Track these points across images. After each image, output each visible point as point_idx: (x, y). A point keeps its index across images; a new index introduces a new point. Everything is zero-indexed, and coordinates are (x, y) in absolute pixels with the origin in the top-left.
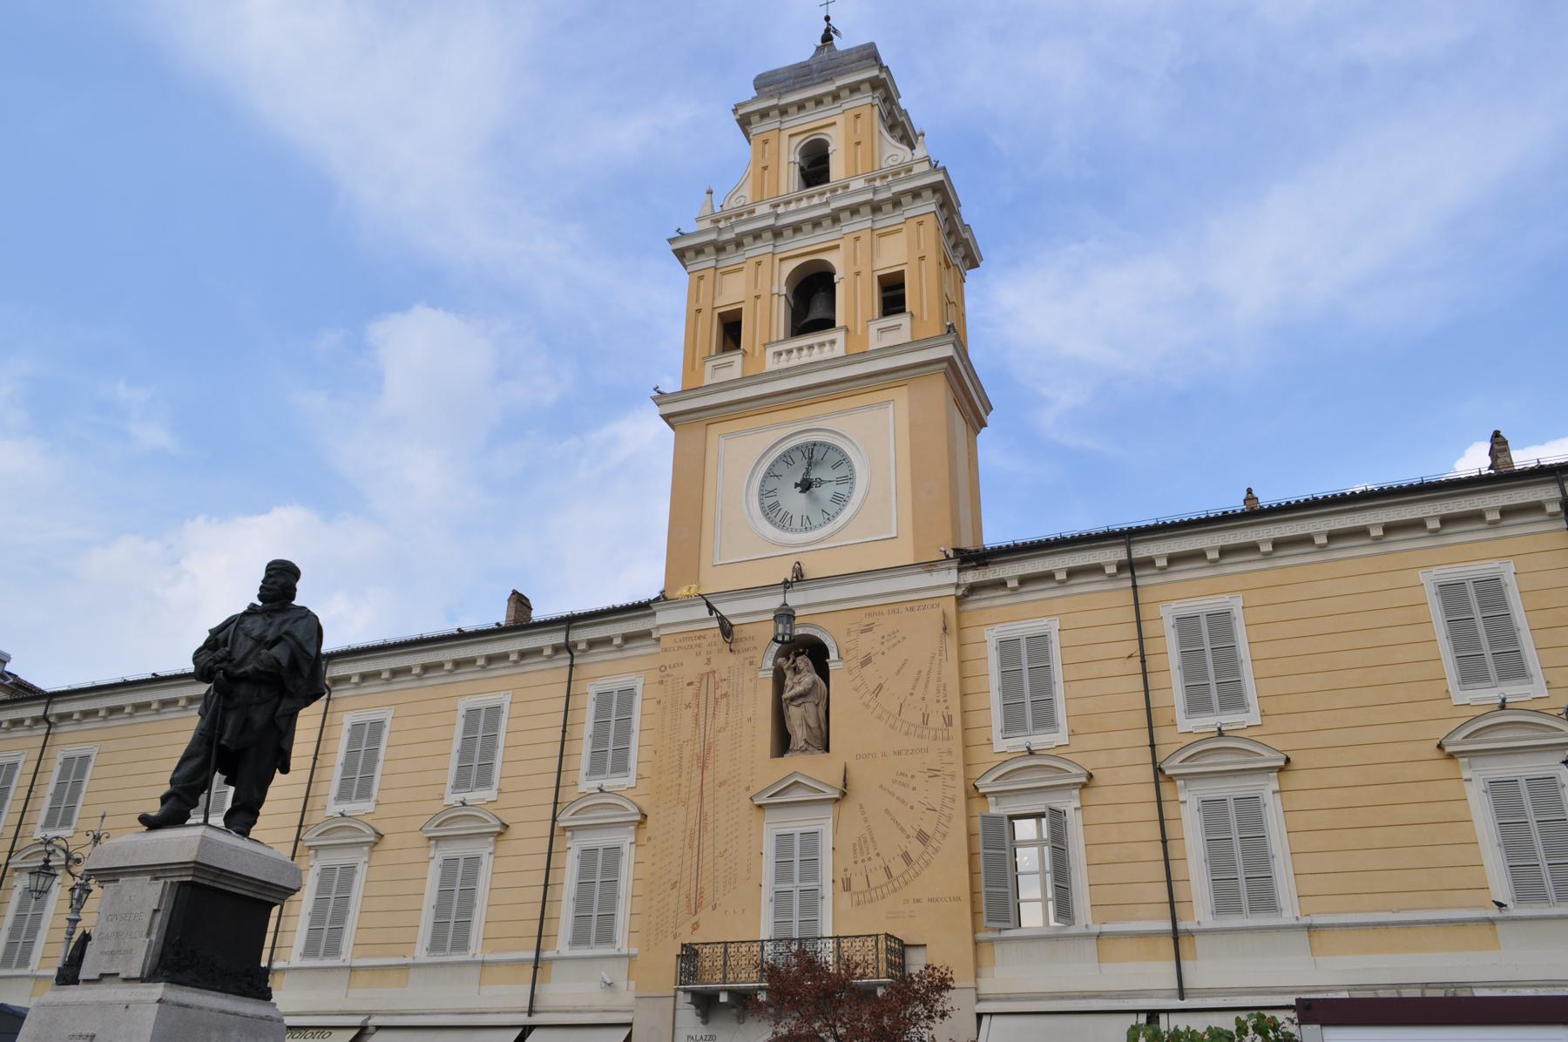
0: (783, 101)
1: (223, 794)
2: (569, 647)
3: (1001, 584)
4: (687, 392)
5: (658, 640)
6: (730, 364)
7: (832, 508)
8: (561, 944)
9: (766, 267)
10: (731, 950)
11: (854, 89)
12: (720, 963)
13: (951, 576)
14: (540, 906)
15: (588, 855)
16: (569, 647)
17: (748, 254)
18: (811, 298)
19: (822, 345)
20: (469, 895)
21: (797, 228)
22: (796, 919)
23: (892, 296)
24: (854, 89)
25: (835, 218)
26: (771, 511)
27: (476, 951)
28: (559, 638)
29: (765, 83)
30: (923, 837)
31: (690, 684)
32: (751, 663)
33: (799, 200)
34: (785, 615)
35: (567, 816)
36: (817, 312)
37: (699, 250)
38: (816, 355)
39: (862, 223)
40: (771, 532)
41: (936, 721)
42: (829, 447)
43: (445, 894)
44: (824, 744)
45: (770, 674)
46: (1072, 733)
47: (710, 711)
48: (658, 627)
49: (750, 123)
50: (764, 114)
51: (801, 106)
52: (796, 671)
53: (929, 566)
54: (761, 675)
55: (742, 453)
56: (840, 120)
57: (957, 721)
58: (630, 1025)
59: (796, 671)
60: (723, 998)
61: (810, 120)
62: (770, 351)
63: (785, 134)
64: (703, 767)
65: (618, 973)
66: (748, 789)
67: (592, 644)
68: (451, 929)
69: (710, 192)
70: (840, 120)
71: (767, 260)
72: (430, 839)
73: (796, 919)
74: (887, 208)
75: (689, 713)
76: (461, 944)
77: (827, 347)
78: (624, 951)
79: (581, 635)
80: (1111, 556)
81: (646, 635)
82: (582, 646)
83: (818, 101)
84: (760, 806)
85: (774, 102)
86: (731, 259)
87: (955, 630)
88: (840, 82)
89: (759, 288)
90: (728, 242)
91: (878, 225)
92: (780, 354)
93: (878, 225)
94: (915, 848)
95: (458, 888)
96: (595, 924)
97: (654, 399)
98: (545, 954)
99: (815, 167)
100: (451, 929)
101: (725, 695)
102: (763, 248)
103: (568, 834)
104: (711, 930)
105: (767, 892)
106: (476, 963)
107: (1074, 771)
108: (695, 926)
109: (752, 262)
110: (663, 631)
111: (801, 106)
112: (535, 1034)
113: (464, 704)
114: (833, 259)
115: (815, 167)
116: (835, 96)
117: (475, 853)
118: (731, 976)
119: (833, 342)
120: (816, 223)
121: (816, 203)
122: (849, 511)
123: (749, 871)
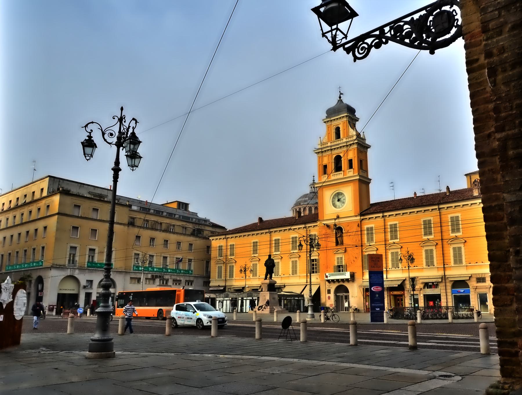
1: (268, 276)
2: (305, 227)
3: (366, 219)
9: (330, 157)
13: (359, 218)
16: (305, 227)
20: (296, 266)
24: (343, 117)
26: (334, 205)
27: (298, 274)
30: (356, 258)
34: (335, 225)
39: (345, 149)
41: (358, 241)
43: (293, 266)
44: (342, 243)
51: (334, 120)
53: (356, 216)
62: (332, 174)
67: (309, 227)
68: (294, 272)
80: (381, 215)
86: (324, 154)
87: (360, 225)
89: (329, 160)
94: (355, 259)
100: (294, 272)
102: (329, 152)
114: (342, 155)
116: (340, 118)
122: (345, 205)
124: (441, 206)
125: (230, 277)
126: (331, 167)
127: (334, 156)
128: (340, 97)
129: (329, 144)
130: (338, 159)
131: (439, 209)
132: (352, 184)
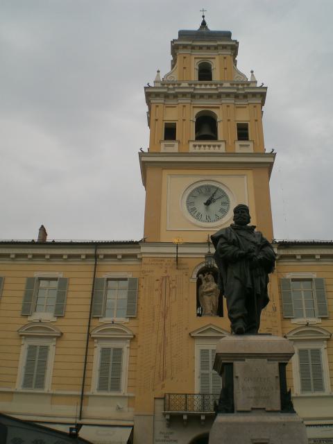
2: (96, 257)
3: (294, 257)
4: (150, 154)
5: (141, 259)
6: (173, 146)
7: (220, 214)
8: (93, 388)
10: (189, 397)
11: (224, 47)
12: (184, 403)
14: (83, 372)
15: (105, 352)
17: (180, 101)
18: (206, 126)
19: (214, 146)
20: (43, 364)
21: (202, 96)
22: (211, 386)
23: (243, 132)
24: (224, 47)
25: (219, 96)
26: (192, 211)
27: (48, 388)
28: (91, 251)
29: (183, 34)
31: (158, 280)
32: (186, 275)
33: (196, 85)
35: (95, 332)
36: (206, 132)
37: (157, 95)
38: (212, 150)
39: (231, 101)
40: (193, 220)
42: (218, 188)
43: (30, 362)
45: (195, 281)
47: (167, 294)
48: (141, 253)
49: (178, 49)
50: (185, 47)
51: (201, 48)
54: (191, 280)
55: (177, 186)
56: (217, 57)
57: (278, 308)
58: (133, 427)
60: (185, 417)
61: (205, 54)
62: (191, 144)
63: (193, 57)
64: (165, 317)
65: (123, 404)
66: (186, 329)
67: (106, 256)
68: (35, 377)
69: (158, 72)
70: (217, 57)
71: (188, 106)
72: (21, 336)
73: (211, 386)
74: (241, 97)
76: (40, 384)
77: (217, 148)
78: (126, 395)
79: (102, 252)
81: (135, 256)
82: (101, 257)
83: (208, 48)
84: (193, 337)
88: (219, 43)
89: (184, 116)
90: (171, 94)
91: (236, 103)
92: (195, 146)
93: (236, 103)
95: (37, 361)
96: (110, 380)
97: (139, 153)
98: (86, 393)
99: (205, 73)
100: (35, 377)
101: (174, 287)
102: (187, 101)
103: (96, 341)
104: (172, 387)
105: (197, 374)
106: (49, 394)
107: (325, 333)
108: (163, 386)
109: (181, 105)
110: (143, 256)
111: (201, 48)
112: (83, 426)
115: (205, 73)
116: (216, 48)
117: (47, 344)
118: (189, 408)
119: (219, 146)
120: (210, 96)
121: (204, 87)
123: (188, 363)
126: (187, 130)
127: (198, 110)
132: (250, 173)
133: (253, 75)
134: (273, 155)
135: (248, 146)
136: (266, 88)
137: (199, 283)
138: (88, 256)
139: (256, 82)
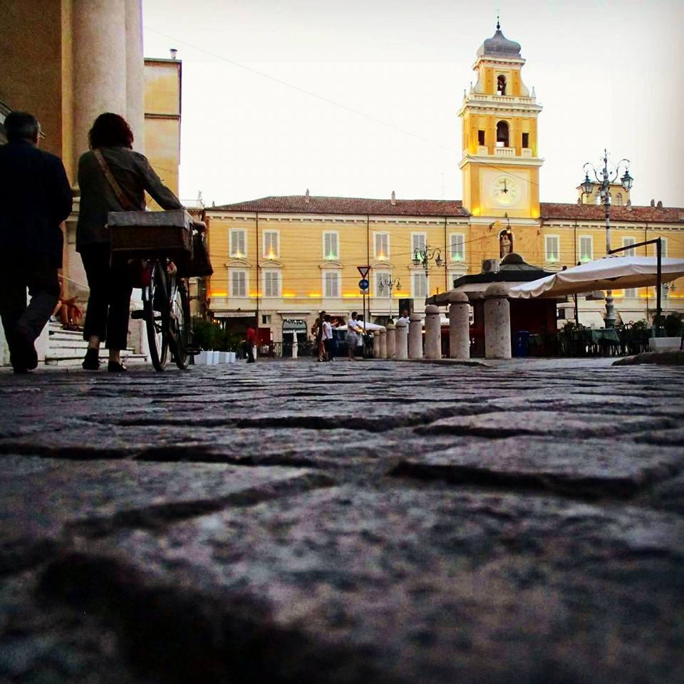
0: (496, 60)
3: (549, 225)
36: (502, 136)
39: (519, 115)
46: (561, 260)
51: (500, 62)
52: (505, 238)
59: (505, 238)
75: (480, 245)
81: (467, 223)
85: (494, 59)
102: (491, 113)
113: (413, 233)
124: (649, 226)
125: (268, 292)
127: (499, 120)
128: (498, 27)
129: (490, 99)
130: (503, 127)
131: (576, 226)
133: (533, 92)
134: (542, 161)
135: (528, 152)
136: (542, 107)
137: (501, 239)
138: (440, 223)
139: (535, 98)
